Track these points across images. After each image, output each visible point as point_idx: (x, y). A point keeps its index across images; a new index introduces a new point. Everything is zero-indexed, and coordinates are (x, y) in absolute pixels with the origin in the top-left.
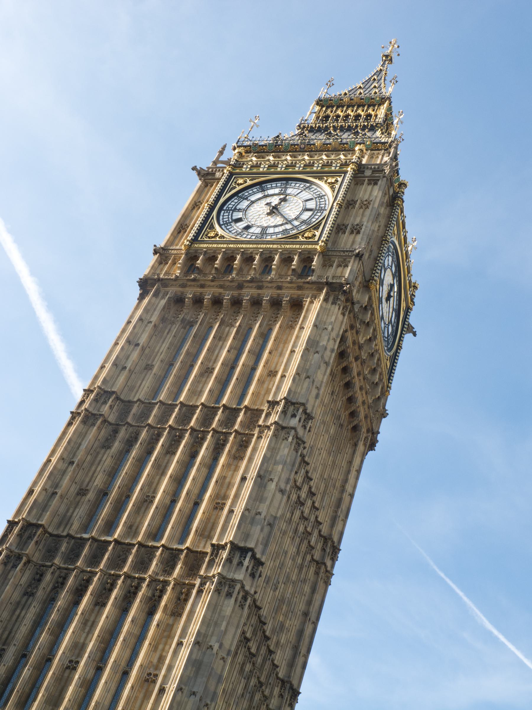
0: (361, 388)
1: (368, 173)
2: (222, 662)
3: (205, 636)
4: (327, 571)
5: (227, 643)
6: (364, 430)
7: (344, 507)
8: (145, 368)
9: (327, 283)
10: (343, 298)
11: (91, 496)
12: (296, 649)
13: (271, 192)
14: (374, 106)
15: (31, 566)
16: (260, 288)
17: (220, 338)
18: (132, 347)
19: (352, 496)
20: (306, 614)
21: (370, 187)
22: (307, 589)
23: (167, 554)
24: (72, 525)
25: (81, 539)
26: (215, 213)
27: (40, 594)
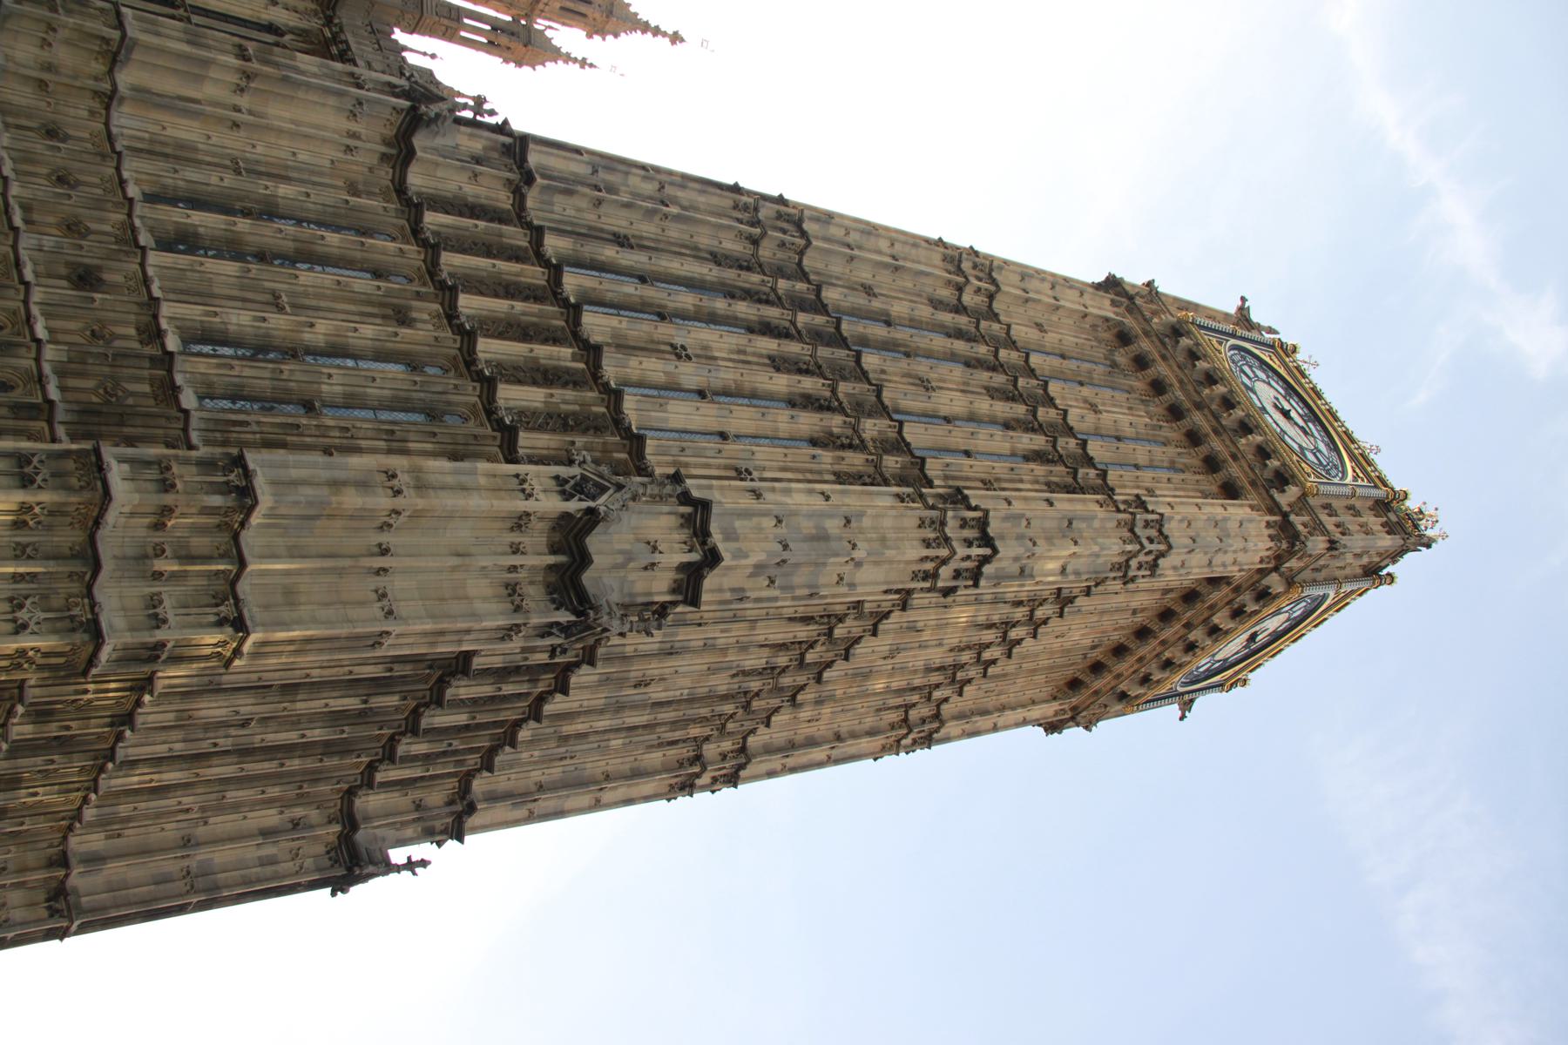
0: (1141, 659)
2: (836, 578)
4: (898, 741)
6: (1074, 701)
7: (981, 722)
8: (1037, 324)
11: (876, 304)
12: (791, 746)
16: (1216, 432)
19: (995, 729)
22: (869, 722)
23: (892, 434)
26: (1233, 341)
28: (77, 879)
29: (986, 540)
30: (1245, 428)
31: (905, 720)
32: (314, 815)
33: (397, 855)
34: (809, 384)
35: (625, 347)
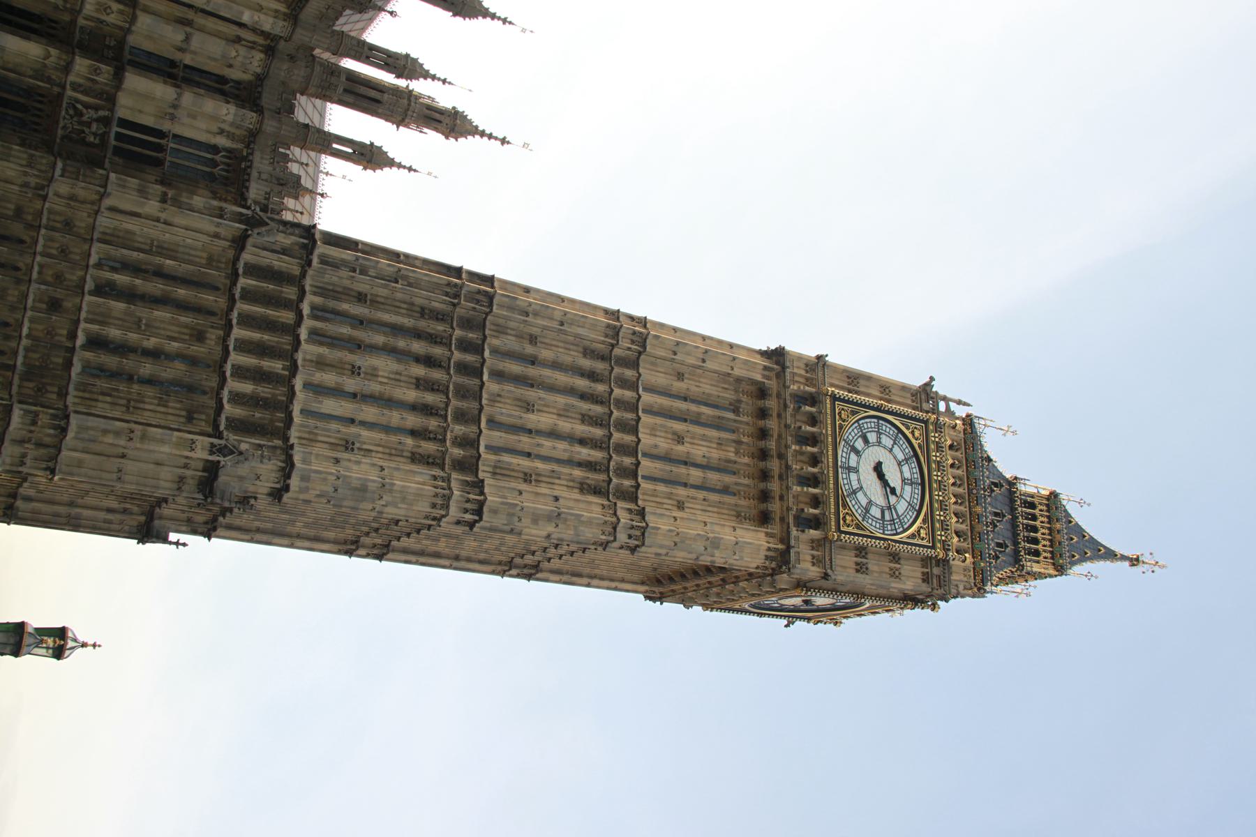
1: (936, 571)
3: (391, 491)
5: (389, 510)
6: (661, 590)
7: (575, 579)
9: (789, 547)
10: (774, 565)
11: (529, 350)
13: (905, 468)
14: (1052, 558)
15: (450, 308)
16: (780, 477)
17: (720, 444)
18: (701, 356)
19: (588, 585)
20: (457, 558)
21: (919, 575)
22: (482, 556)
23: (473, 436)
24: (497, 337)
25: (483, 350)
26: (872, 413)
27: (422, 324)
28: (19, 503)
29: (479, 512)
30: (814, 481)
31: (511, 562)
32: (135, 509)
33: (173, 537)
34: (430, 398)
35: (321, 364)
